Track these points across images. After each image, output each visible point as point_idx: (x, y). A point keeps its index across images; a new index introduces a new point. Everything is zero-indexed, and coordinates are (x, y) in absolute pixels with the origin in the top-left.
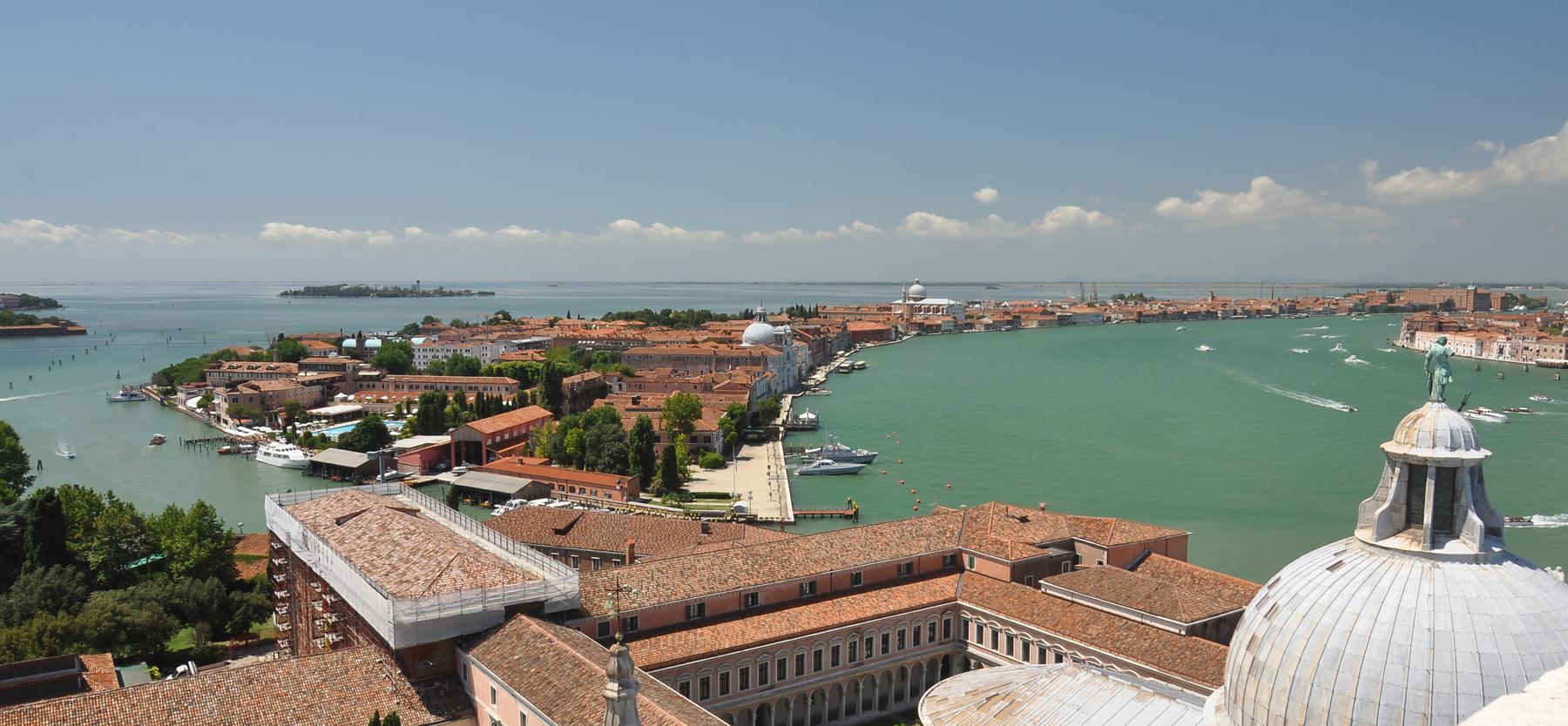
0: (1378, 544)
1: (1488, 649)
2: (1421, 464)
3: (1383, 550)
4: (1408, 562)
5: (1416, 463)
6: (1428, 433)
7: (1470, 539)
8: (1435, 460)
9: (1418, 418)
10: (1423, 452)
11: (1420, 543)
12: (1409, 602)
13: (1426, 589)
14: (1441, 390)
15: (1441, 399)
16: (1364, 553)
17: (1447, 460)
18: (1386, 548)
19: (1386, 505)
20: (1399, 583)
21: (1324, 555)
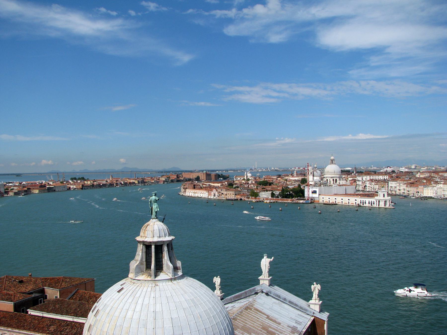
0: (136, 279)
1: (175, 316)
2: (149, 244)
3: (138, 281)
4: (147, 284)
5: (148, 244)
6: (151, 232)
7: (169, 273)
8: (154, 242)
9: (148, 226)
10: (149, 239)
11: (151, 276)
12: (146, 302)
13: (153, 295)
14: (155, 214)
15: (155, 217)
16: (131, 283)
17: (158, 242)
18: (139, 280)
19: (138, 263)
20: (143, 294)
21: (117, 286)
